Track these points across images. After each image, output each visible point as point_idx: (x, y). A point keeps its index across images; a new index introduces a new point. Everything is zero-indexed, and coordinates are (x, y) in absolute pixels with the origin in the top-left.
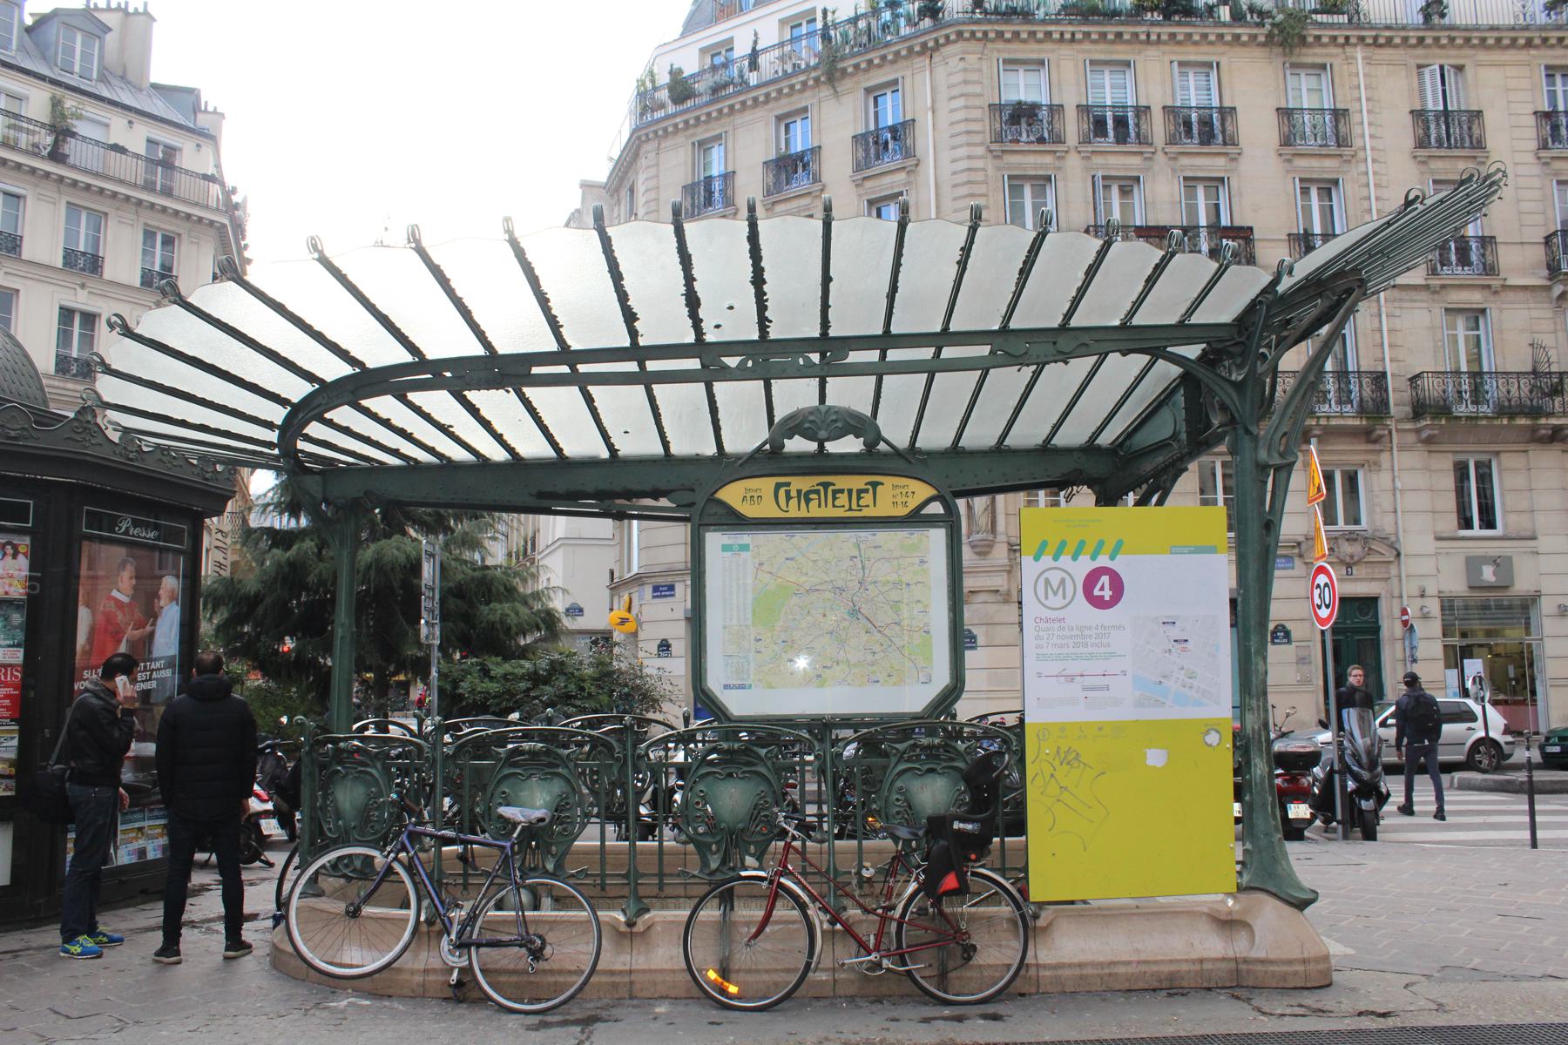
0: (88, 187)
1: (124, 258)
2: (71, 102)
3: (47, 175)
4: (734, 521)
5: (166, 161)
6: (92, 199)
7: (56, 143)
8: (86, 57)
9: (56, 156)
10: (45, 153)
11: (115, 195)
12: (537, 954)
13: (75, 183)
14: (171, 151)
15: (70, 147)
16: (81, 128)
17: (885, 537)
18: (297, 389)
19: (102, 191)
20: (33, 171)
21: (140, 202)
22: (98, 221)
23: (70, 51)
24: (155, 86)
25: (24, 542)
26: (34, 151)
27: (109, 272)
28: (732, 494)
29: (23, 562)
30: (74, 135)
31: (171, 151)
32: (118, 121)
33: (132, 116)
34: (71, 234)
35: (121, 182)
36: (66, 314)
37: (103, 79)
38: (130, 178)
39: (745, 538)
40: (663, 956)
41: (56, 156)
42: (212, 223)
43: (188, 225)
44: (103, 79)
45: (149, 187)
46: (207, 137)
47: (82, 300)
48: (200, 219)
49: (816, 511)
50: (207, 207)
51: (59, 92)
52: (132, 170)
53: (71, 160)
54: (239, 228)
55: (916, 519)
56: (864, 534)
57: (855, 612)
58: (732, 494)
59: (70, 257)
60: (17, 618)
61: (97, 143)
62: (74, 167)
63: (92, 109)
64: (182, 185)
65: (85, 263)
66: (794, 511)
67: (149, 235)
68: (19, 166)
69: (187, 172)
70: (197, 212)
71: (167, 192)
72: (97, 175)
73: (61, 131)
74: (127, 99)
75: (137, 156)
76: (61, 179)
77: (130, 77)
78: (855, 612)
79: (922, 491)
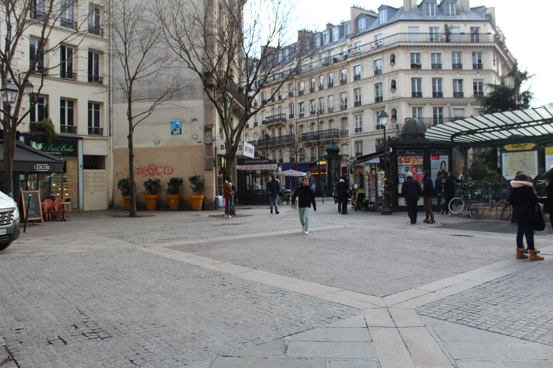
0: (456, 46)
1: (468, 62)
2: (449, 25)
3: (446, 46)
4: (506, 151)
5: (475, 33)
6: (457, 50)
7: (447, 38)
8: (452, 10)
9: (448, 41)
10: (445, 40)
11: (463, 46)
12: (477, 211)
13: (453, 46)
14: (477, 28)
15: (451, 37)
16: (453, 31)
17: (528, 153)
18: (450, 136)
19: (460, 46)
20: (442, 46)
21: (470, 46)
22: (459, 54)
23: (448, 10)
24: (472, 9)
25: (422, 156)
26: (442, 41)
27: (464, 68)
28: (506, 147)
29: (422, 159)
30: (451, 34)
31: (477, 28)
32: (462, 25)
33: (466, 23)
34: (453, 60)
35: (464, 42)
36: (454, 81)
37: (458, 13)
38: (466, 40)
39: (508, 154)
40: (494, 213)
41: (448, 41)
42: (491, 46)
43: (484, 49)
44: (458, 13)
45: (472, 41)
46: (490, 19)
47: (458, 76)
48: (487, 46)
49: (518, 149)
50: (489, 42)
51: (446, 23)
52: (469, 38)
53: (451, 41)
54: (501, 44)
55: (533, 149)
56: (525, 152)
57: (524, 164)
58: (506, 147)
59: (454, 66)
60: (422, 167)
61: (457, 34)
62: (452, 42)
63: (455, 25)
64: (481, 38)
65: (457, 67)
66: (515, 149)
67: (474, 54)
68: (439, 46)
69: (482, 34)
70: (486, 44)
71: (478, 41)
72: (458, 43)
73: (448, 33)
74: (464, 17)
75: (468, 34)
76: (449, 46)
77: (465, 10)
78: (524, 164)
79: (533, 145)
